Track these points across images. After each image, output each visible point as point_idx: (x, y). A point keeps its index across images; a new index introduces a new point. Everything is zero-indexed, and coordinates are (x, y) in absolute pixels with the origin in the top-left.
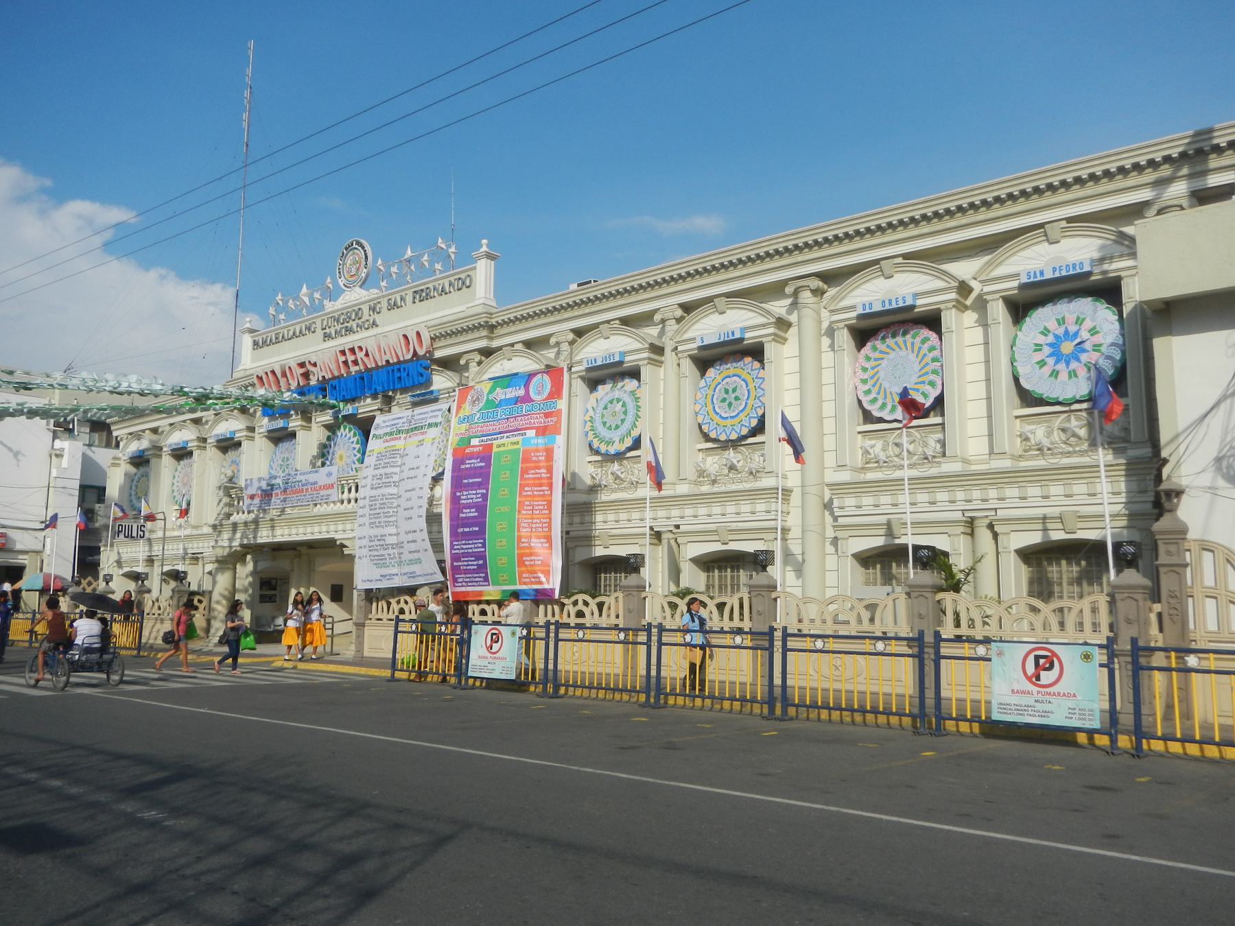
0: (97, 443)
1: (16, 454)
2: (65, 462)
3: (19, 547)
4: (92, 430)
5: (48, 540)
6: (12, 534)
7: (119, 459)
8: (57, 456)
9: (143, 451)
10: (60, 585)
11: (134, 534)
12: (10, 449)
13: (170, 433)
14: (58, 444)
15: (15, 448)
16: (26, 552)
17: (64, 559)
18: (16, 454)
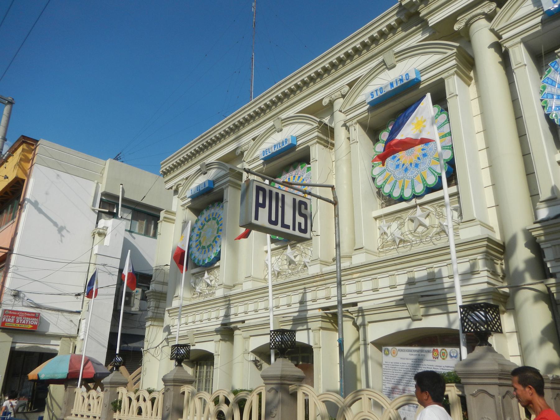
0: (137, 230)
1: (61, 229)
2: (107, 241)
3: (52, 330)
4: (134, 218)
5: (83, 322)
6: (46, 315)
7: (174, 213)
8: (100, 234)
9: (213, 182)
10: (92, 371)
11: (288, 221)
12: (55, 224)
13: (255, 148)
14: (103, 223)
15: (60, 224)
16: (58, 337)
17: (100, 344)
18: (61, 229)
